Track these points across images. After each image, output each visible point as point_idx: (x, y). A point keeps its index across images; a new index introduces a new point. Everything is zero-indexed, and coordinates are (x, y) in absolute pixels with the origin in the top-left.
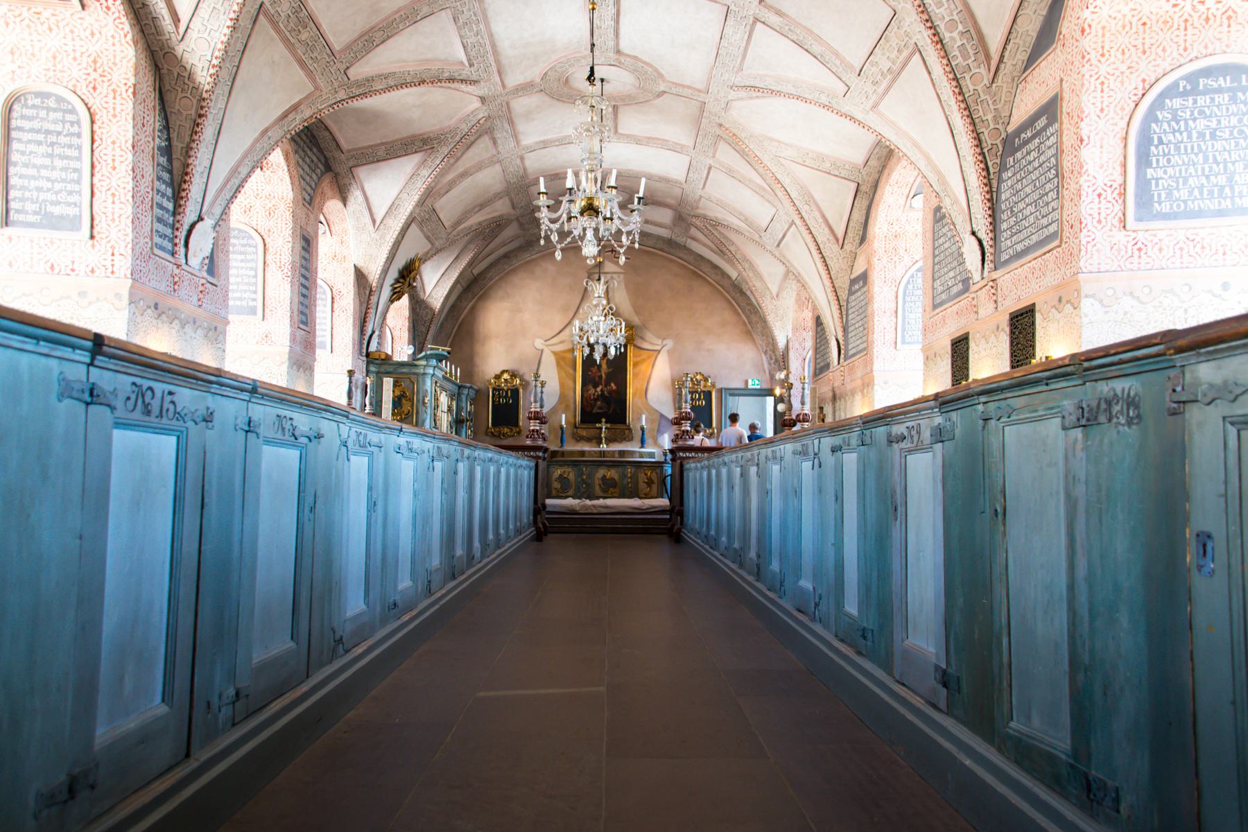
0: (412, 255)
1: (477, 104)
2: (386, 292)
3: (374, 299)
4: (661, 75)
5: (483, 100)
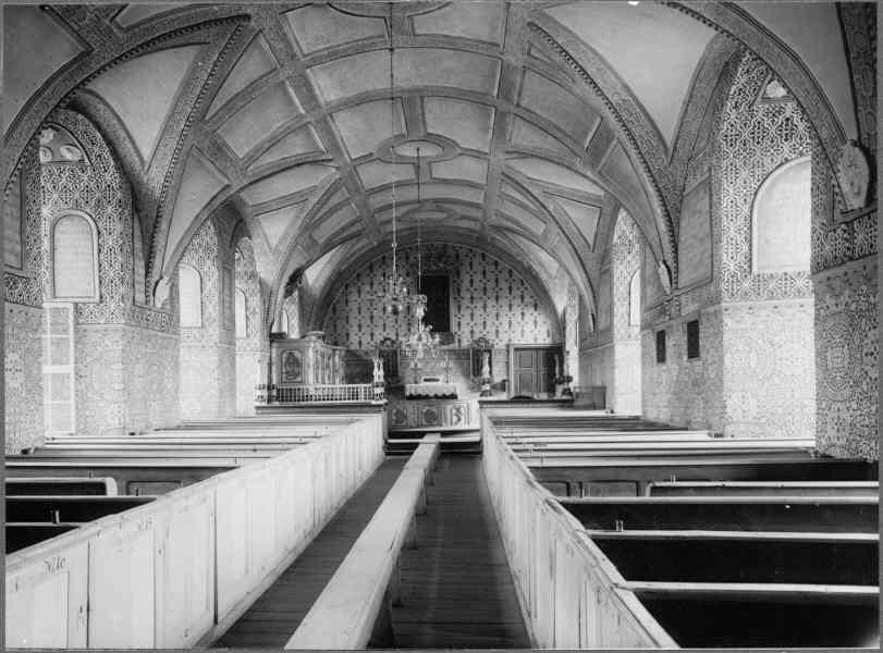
0: (297, 266)
1: (334, 170)
2: (282, 291)
3: (273, 299)
4: (457, 145)
5: (338, 168)
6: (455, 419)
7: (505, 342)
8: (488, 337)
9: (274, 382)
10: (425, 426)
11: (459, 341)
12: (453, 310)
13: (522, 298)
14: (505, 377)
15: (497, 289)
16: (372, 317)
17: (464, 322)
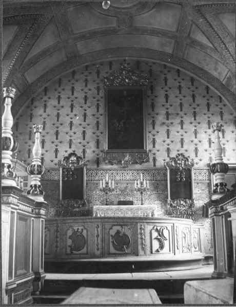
6: (156, 245)
8: (186, 155)
10: (115, 255)
11: (154, 160)
13: (221, 114)
15: (194, 105)
16: (57, 133)
17: (159, 140)
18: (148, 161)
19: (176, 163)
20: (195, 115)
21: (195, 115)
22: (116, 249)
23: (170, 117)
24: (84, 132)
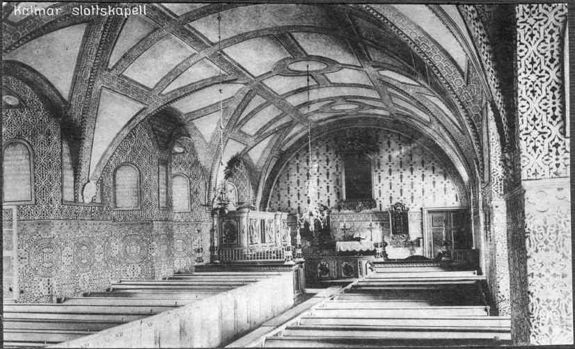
7: (419, 206)
9: (216, 245)
10: (345, 278)
12: (375, 178)
14: (420, 236)
17: (383, 192)
18: (375, 207)
19: (395, 209)
20: (412, 170)
21: (412, 170)
22: (345, 274)
23: (392, 172)
24: (328, 187)
